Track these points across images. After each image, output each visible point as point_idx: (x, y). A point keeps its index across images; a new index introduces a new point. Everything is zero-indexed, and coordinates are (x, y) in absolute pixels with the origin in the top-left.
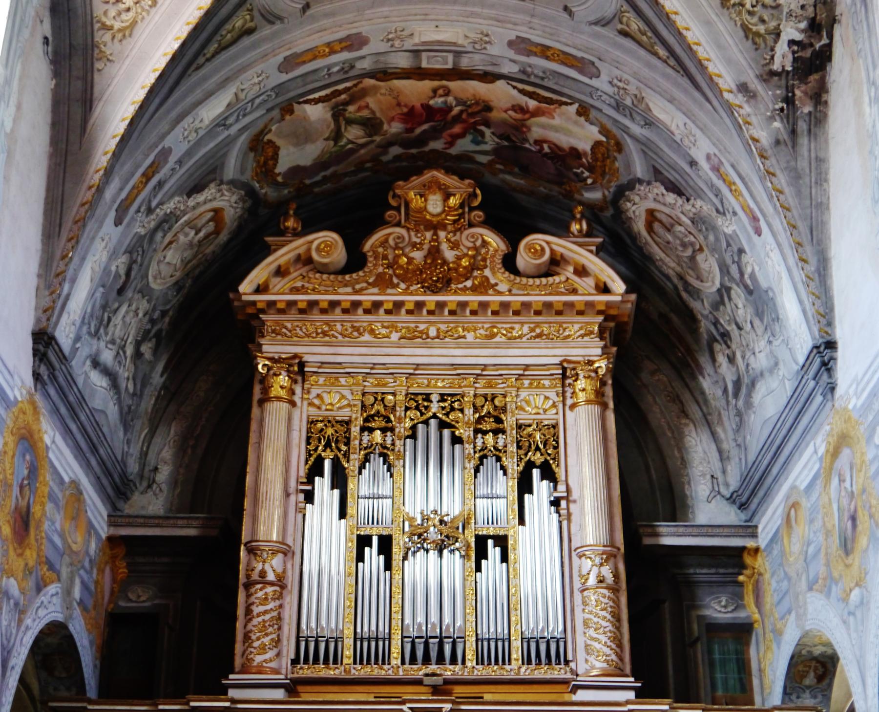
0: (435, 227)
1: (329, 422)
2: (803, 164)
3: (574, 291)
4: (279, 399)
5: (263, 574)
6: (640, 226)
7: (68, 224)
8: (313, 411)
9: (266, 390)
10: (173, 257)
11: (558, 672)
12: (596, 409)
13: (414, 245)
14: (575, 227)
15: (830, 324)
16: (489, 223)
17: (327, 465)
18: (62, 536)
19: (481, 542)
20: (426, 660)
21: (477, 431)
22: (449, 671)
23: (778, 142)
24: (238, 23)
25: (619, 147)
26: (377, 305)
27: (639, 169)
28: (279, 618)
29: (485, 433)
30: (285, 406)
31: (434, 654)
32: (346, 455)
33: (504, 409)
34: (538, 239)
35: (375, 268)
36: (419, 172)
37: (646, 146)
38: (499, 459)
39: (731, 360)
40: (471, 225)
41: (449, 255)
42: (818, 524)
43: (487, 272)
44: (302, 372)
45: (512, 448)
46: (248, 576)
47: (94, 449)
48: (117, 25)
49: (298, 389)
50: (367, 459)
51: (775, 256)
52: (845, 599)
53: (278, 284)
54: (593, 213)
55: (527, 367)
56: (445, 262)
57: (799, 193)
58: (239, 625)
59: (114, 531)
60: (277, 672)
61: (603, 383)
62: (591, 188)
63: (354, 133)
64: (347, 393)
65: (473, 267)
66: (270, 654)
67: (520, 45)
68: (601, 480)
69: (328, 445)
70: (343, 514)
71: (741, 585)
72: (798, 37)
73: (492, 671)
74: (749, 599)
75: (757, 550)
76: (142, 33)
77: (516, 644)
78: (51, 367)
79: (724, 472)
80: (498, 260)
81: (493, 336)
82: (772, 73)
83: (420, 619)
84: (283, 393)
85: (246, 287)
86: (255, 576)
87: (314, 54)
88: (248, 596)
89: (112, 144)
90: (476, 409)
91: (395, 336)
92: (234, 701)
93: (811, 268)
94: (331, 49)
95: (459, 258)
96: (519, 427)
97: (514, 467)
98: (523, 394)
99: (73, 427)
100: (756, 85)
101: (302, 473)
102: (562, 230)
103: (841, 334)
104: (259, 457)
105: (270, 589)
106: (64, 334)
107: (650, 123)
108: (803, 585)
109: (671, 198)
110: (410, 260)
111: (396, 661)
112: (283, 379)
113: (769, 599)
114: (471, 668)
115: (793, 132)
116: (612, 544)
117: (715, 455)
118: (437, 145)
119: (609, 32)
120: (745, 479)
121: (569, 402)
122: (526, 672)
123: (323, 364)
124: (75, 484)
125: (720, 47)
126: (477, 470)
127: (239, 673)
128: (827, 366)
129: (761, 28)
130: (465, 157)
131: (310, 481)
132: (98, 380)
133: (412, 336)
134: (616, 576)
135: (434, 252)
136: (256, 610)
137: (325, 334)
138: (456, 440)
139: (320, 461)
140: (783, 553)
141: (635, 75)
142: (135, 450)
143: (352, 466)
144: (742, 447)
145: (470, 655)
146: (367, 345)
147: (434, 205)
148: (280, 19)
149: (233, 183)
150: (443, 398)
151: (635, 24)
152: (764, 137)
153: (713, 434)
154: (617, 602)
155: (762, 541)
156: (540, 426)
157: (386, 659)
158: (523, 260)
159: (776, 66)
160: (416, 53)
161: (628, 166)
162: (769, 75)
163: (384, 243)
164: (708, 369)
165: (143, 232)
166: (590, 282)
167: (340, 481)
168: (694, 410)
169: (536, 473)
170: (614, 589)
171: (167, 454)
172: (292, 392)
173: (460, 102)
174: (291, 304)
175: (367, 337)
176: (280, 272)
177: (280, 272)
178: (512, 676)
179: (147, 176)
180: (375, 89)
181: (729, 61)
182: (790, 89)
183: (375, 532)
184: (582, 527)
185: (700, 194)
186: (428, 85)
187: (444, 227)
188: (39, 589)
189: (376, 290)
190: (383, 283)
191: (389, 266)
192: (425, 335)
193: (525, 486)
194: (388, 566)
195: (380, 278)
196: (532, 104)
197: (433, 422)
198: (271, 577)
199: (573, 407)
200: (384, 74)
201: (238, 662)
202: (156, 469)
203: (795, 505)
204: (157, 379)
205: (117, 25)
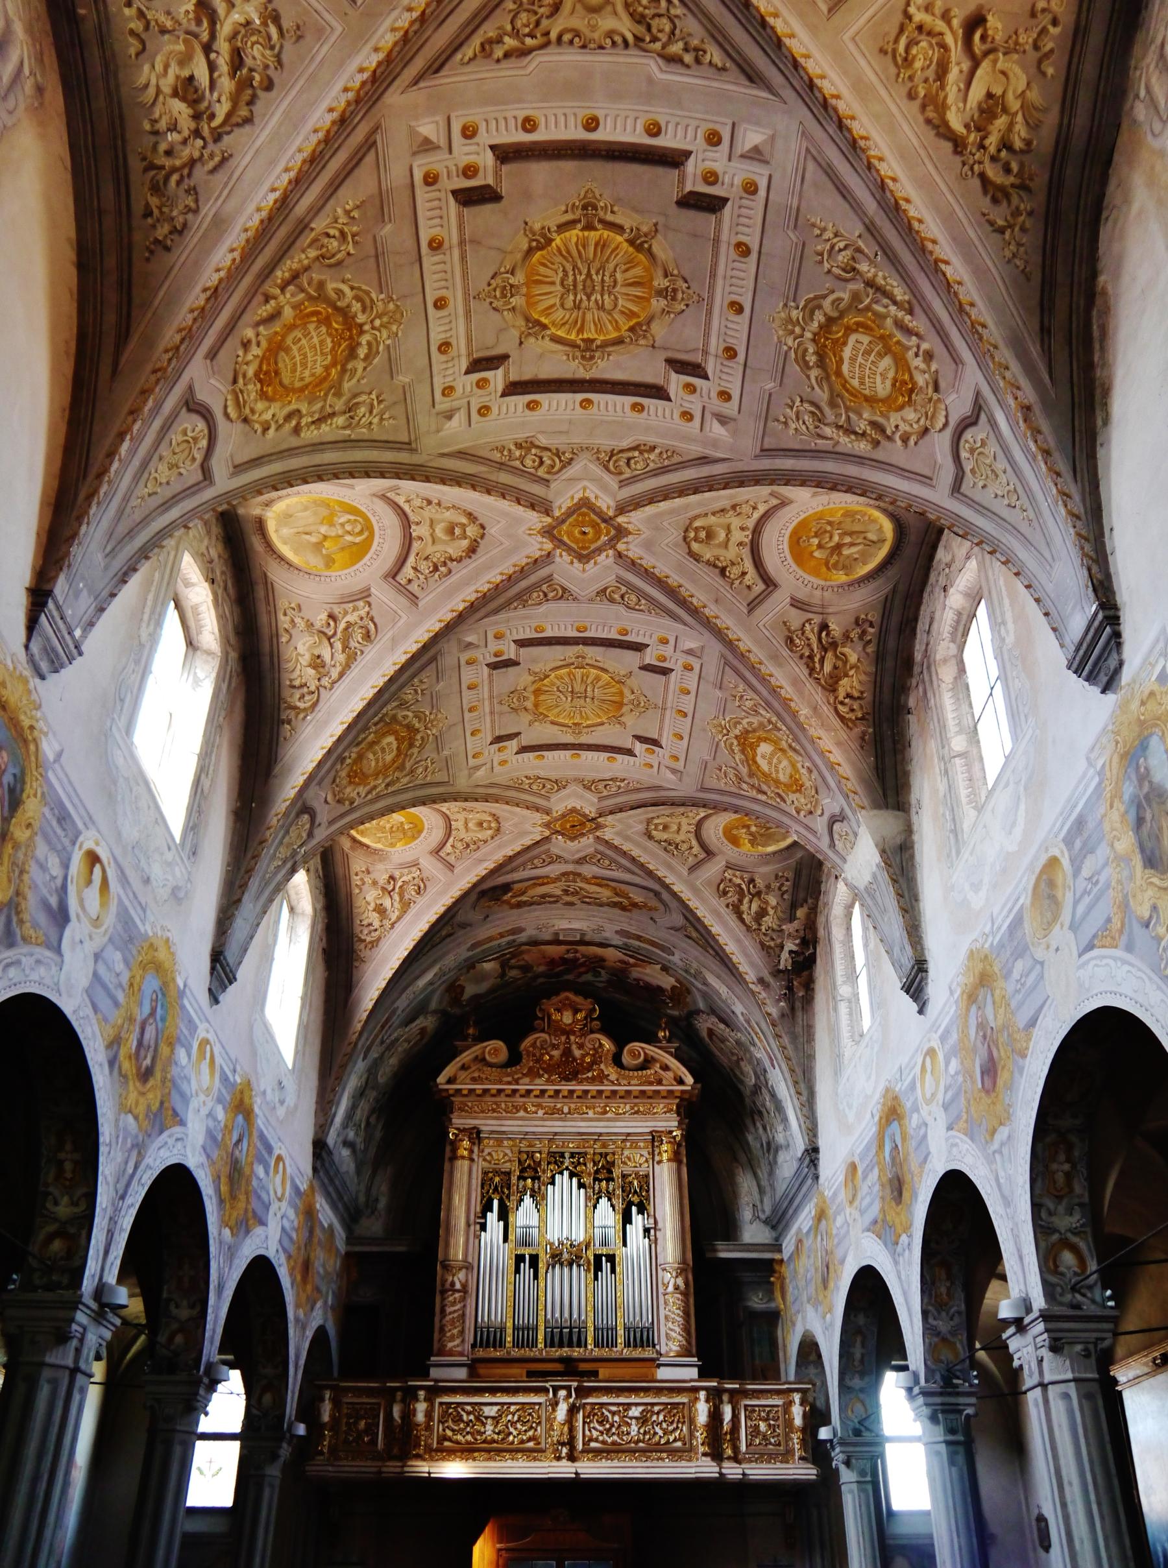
0: (568, 1032)
1: (497, 1172)
2: (799, 1029)
3: (660, 1082)
4: (463, 1157)
5: (453, 1284)
6: (704, 1034)
7: (335, 1069)
8: (486, 1164)
9: (454, 1150)
10: (393, 1061)
11: (649, 1353)
12: (674, 1165)
13: (555, 1047)
14: (661, 1034)
15: (815, 1136)
16: (604, 1031)
17: (496, 1203)
18: (324, 1266)
19: (598, 1258)
20: (561, 1345)
21: (595, 1179)
22: (577, 1353)
23: (783, 1015)
24: (444, 933)
25: (689, 992)
26: (529, 1092)
27: (701, 1005)
28: (464, 1315)
29: (600, 1181)
30: (466, 1163)
31: (566, 1340)
32: (508, 1197)
33: (613, 1164)
34: (636, 1045)
35: (527, 1063)
36: (557, 994)
37: (705, 996)
38: (610, 1199)
39: (765, 1128)
40: (592, 1032)
41: (577, 1053)
42: (812, 1260)
43: (602, 1066)
44: (479, 1138)
45: (619, 1192)
46: (443, 1285)
47: (341, 1198)
48: (368, 939)
49: (476, 1149)
50: (522, 1200)
51: (783, 1084)
52: (824, 1318)
53: (463, 1075)
54: (673, 1023)
55: (629, 1134)
56: (575, 1059)
57: (796, 1049)
58: (437, 1319)
59: (351, 1249)
60: (461, 1354)
61: (679, 1145)
62: (671, 1008)
63: (514, 973)
64: (508, 1151)
65: (593, 1063)
66: (457, 1342)
67: (621, 933)
68: (677, 1216)
69: (496, 1190)
70: (506, 1239)
71: (772, 1284)
72: (795, 948)
73: (605, 1353)
74: (778, 1295)
75: (782, 1261)
76: (384, 946)
77: (621, 1332)
78: (323, 1160)
79: (762, 1201)
80: (610, 1057)
81: (605, 1112)
82: (780, 971)
83: (557, 1315)
84: (466, 1153)
85: (441, 1079)
86: (448, 1286)
87: (491, 939)
88: (443, 1299)
89: (365, 1015)
90: (595, 1164)
91: (541, 1113)
92: (436, 1381)
93: (804, 1098)
94: (502, 935)
95: (584, 1056)
96: (624, 1176)
97: (620, 1206)
98: (626, 1153)
99: (331, 1189)
100: (769, 979)
101: (479, 1209)
102: (651, 1039)
103: (822, 1143)
104: (450, 1199)
105: (457, 1295)
106: (331, 1139)
107: (706, 984)
108: (805, 1298)
109: (722, 1026)
110: (551, 1057)
111: (541, 1346)
112: (466, 1143)
113: (790, 1298)
114: (591, 1349)
115: (793, 1009)
116: (684, 1261)
117: (755, 1190)
118: (570, 977)
119: (679, 934)
120: (774, 1211)
121: (657, 1158)
122: (626, 1353)
123: (492, 1132)
124: (331, 1226)
125: (746, 955)
126: (595, 1207)
127: (438, 1355)
128: (814, 1163)
129: (772, 944)
130: (588, 983)
131: (484, 1217)
132: (346, 1152)
133: (553, 1112)
134: (686, 1284)
135: (567, 1052)
136: (449, 1310)
137: (494, 1111)
138: (581, 1186)
139: (490, 1201)
140: (795, 1271)
141: (696, 959)
142: (363, 1188)
143: (511, 1204)
144: (772, 1186)
145: (590, 1340)
146: (521, 1119)
147: (567, 1018)
148: (470, 925)
149: (435, 1012)
150: (572, 1155)
151: (694, 934)
152: (774, 1011)
153: (755, 1175)
154: (686, 1302)
155: (786, 1255)
156: (637, 1176)
157: (535, 1343)
158: (626, 1059)
159: (782, 967)
160: (557, 934)
161: (695, 1002)
162: (777, 973)
163: (534, 1045)
164: (752, 1129)
165: (376, 1055)
166: (670, 1075)
167: (503, 1216)
168: (743, 1158)
169: (634, 1209)
170: (685, 1294)
171: (384, 1188)
172: (471, 1151)
173: (583, 956)
174: (471, 1091)
175: (522, 1113)
176: (464, 1067)
177: (464, 1067)
178: (617, 1356)
179: (383, 1027)
180: (528, 951)
181: (752, 964)
182: (790, 981)
183: (527, 1252)
184: (664, 1249)
185: (739, 1030)
186: (563, 948)
187: (574, 1033)
188: (312, 1309)
189: (527, 1080)
190: (533, 1074)
191: (537, 1061)
192: (561, 1111)
193: (627, 1219)
194: (536, 1277)
195: (530, 1069)
196: (632, 961)
197: (566, 1173)
198: (458, 1286)
199: (660, 1162)
200: (535, 943)
201: (436, 1346)
202: (377, 1200)
203: (800, 1241)
204: (378, 1134)
205: (368, 939)
